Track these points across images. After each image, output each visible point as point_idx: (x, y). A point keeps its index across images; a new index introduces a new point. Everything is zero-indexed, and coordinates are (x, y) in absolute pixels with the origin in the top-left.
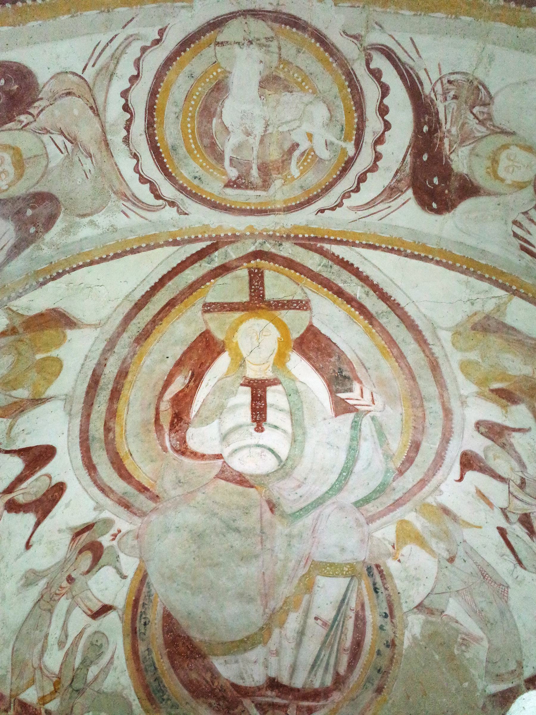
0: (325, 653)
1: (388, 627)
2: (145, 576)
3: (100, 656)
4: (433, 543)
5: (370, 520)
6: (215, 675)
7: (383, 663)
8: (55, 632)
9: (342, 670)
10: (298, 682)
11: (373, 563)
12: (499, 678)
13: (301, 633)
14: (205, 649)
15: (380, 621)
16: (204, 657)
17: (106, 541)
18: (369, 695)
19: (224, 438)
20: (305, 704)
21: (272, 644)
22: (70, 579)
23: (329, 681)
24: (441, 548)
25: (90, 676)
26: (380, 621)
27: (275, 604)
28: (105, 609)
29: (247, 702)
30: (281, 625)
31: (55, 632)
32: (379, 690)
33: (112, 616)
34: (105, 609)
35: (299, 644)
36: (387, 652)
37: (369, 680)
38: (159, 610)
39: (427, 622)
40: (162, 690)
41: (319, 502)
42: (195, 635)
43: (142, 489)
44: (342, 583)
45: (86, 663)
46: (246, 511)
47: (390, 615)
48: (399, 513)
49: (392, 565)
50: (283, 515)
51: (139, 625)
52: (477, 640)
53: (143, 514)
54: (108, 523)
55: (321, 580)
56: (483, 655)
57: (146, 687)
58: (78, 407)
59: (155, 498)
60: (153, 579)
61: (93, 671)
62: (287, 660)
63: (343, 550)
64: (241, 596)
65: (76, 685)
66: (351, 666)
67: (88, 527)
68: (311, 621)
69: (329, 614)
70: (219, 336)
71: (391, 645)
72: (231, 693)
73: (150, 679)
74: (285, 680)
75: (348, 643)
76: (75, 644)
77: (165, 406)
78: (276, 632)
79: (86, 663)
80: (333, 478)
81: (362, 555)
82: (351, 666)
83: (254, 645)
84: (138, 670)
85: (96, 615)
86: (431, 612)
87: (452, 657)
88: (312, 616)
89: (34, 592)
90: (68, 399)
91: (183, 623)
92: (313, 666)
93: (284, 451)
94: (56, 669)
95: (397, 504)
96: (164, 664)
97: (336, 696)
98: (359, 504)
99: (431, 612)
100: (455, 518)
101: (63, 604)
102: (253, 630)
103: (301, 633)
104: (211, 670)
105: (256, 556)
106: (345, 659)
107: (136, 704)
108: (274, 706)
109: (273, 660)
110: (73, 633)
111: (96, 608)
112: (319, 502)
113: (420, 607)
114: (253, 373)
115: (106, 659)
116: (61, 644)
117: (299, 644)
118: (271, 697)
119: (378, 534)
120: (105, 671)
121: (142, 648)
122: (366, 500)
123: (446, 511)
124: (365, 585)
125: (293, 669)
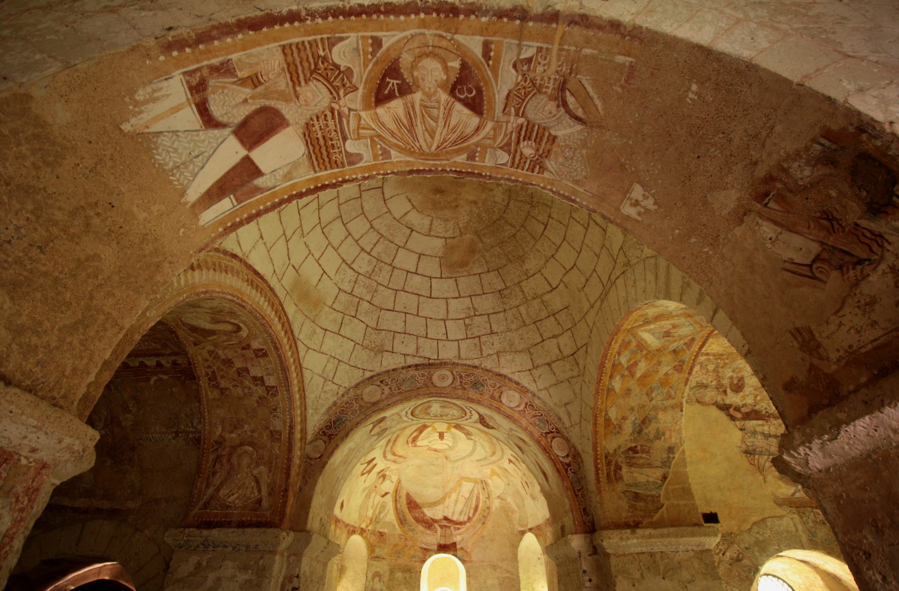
0: (465, 509)
1: (488, 502)
2: (400, 481)
3: (384, 510)
4: (503, 478)
5: (482, 466)
6: (425, 515)
7: (485, 514)
8: (371, 504)
9: (471, 516)
10: (455, 518)
11: (483, 479)
12: (522, 526)
13: (457, 501)
14: (421, 506)
15: (485, 499)
16: (421, 508)
17: (387, 473)
18: (480, 525)
19: (430, 442)
20: (457, 526)
21: (446, 503)
22: (376, 487)
23: (466, 519)
24: (505, 480)
25: (381, 517)
26: (485, 499)
27: (447, 490)
28: (387, 494)
29: (436, 525)
30: (449, 497)
31: (371, 504)
32: (484, 524)
33: (388, 496)
34: (387, 494)
35: (456, 504)
36: (487, 510)
37: (480, 520)
38: (405, 492)
39: (500, 503)
40: (405, 520)
41: (464, 458)
42: (418, 501)
43: (400, 457)
44: (473, 484)
45: (380, 513)
46: (437, 459)
47: (488, 498)
48: (492, 466)
49: (489, 482)
50: (450, 461)
51: (398, 498)
52: (516, 512)
53: (400, 463)
54: (388, 468)
55: (464, 483)
56: (518, 518)
57: (400, 519)
58: (384, 447)
59: (405, 458)
60: (403, 483)
61: (382, 515)
62: (451, 510)
63: (472, 474)
64: (434, 487)
65: (377, 520)
66: (474, 514)
67: (382, 471)
68: (460, 497)
69: (467, 495)
70: (428, 424)
71: (489, 508)
72: (431, 521)
73: (401, 516)
74: (450, 517)
75: (473, 506)
76: (376, 507)
77: (410, 440)
78: (447, 499)
79: (380, 513)
80: (468, 452)
81: (479, 476)
82: (474, 514)
83: (439, 504)
84: (397, 513)
85: (383, 496)
86: (502, 499)
87: (508, 516)
88: (461, 494)
89: (365, 494)
90: (381, 446)
91: (413, 496)
92: (460, 513)
93: (451, 444)
94: (371, 516)
95: (490, 464)
96: (406, 511)
97: (468, 524)
98: (478, 461)
99: (502, 499)
100: (509, 473)
101: (373, 494)
102: (439, 498)
103: (457, 501)
104: (423, 513)
105: (441, 473)
106: (472, 511)
107: (396, 523)
108: (446, 526)
109: (446, 509)
110: (376, 504)
111: (383, 494)
112: (464, 458)
113: (498, 497)
114: (439, 430)
115: (386, 511)
116: (372, 507)
117: (456, 504)
118: (445, 523)
119: (485, 471)
120: (386, 514)
121: (398, 506)
122: (480, 460)
123: (506, 470)
124: (480, 486)
125: (453, 513)
